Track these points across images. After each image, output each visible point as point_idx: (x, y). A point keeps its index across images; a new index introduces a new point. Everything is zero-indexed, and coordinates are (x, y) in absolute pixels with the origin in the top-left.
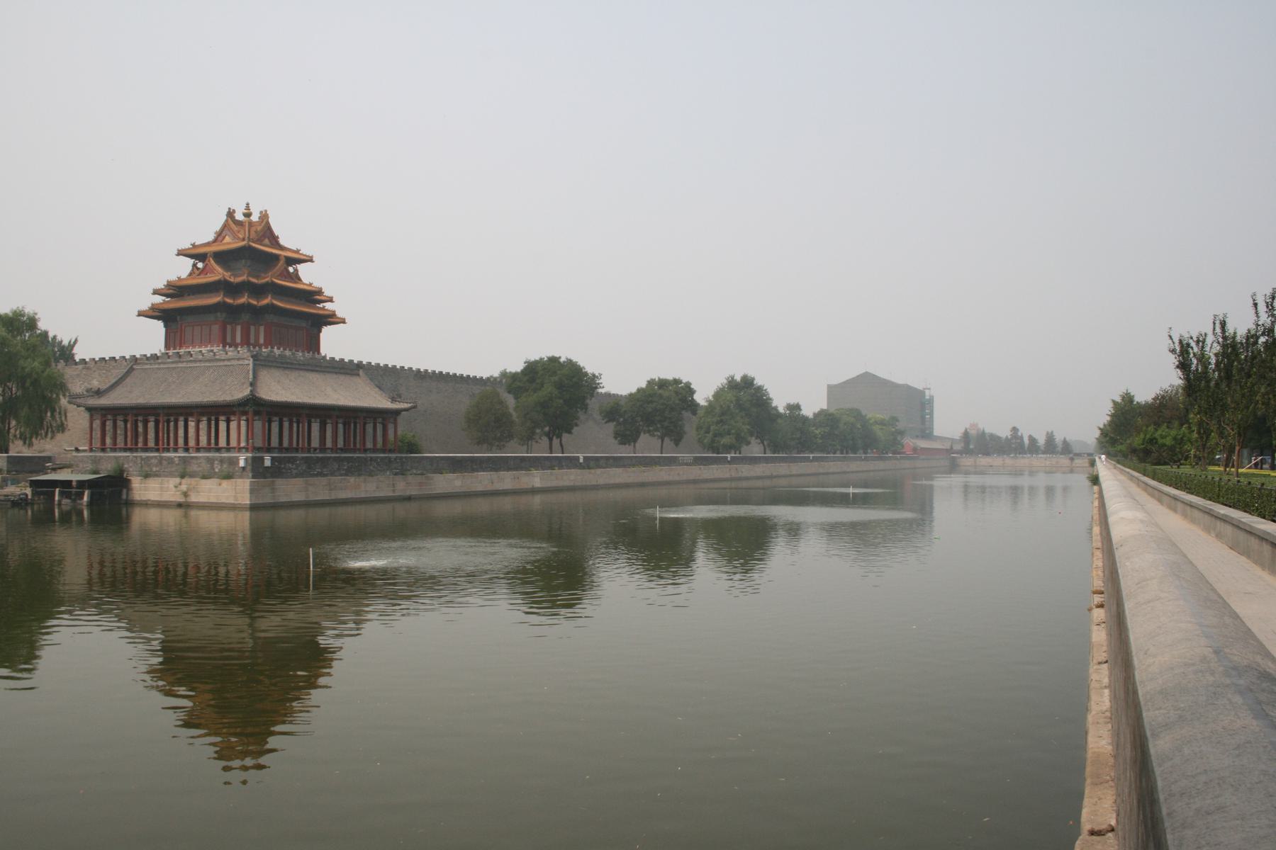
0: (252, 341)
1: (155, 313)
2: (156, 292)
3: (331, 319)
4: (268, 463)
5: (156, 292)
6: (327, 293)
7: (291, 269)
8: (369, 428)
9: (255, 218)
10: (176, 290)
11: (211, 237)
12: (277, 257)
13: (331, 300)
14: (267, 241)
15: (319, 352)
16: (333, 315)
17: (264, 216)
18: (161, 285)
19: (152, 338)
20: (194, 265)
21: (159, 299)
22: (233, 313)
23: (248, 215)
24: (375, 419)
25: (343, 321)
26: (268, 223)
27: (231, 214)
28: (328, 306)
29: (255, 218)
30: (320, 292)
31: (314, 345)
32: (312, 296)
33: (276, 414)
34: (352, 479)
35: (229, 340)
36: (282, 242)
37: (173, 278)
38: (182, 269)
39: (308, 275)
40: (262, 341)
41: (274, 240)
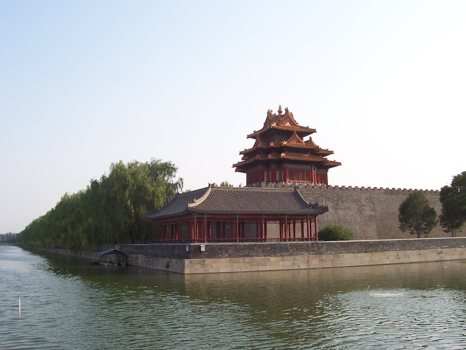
0: (278, 179)
4: (203, 249)
13: (332, 153)
14: (288, 124)
15: (326, 182)
17: (287, 110)
22: (267, 163)
23: (280, 112)
24: (302, 219)
25: (339, 164)
27: (269, 113)
29: (283, 113)
31: (324, 179)
33: (291, 219)
34: (272, 259)
41: (293, 123)
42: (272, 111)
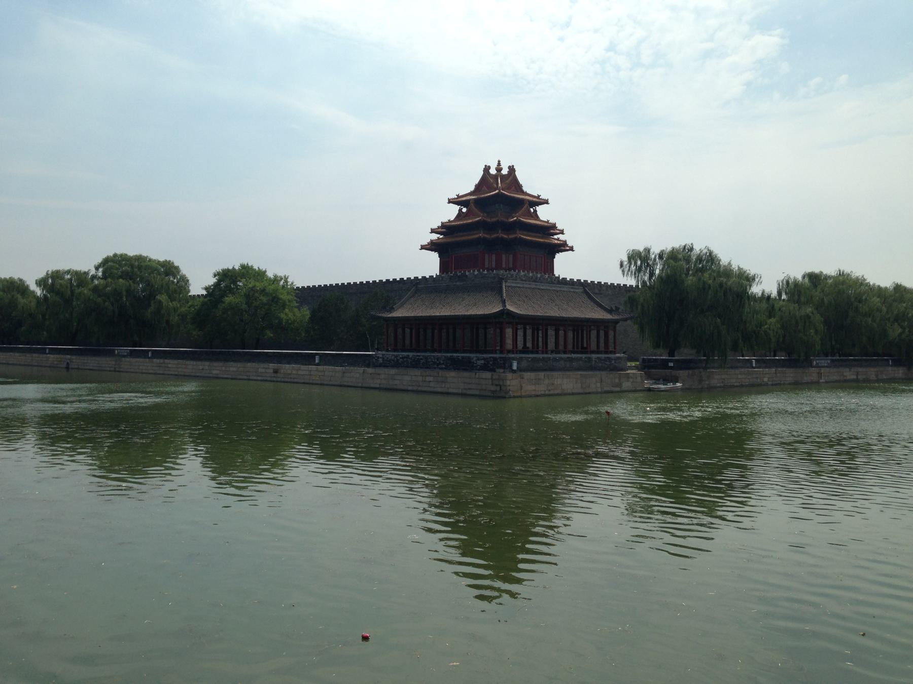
1: (432, 246)
2: (433, 231)
3: (563, 247)
5: (433, 231)
6: (559, 226)
7: (532, 210)
8: (594, 334)
9: (505, 171)
10: (446, 229)
11: (472, 188)
12: (521, 202)
13: (562, 232)
16: (564, 244)
17: (512, 169)
18: (436, 224)
19: (429, 265)
20: (460, 210)
21: (435, 236)
22: (490, 245)
23: (499, 169)
25: (571, 249)
26: (515, 176)
27: (487, 169)
28: (561, 237)
29: (505, 171)
30: (554, 226)
32: (549, 229)
35: (487, 266)
36: (525, 189)
37: (445, 220)
38: (451, 213)
39: (544, 213)
40: (511, 266)
41: (518, 187)
42: (489, 167)
